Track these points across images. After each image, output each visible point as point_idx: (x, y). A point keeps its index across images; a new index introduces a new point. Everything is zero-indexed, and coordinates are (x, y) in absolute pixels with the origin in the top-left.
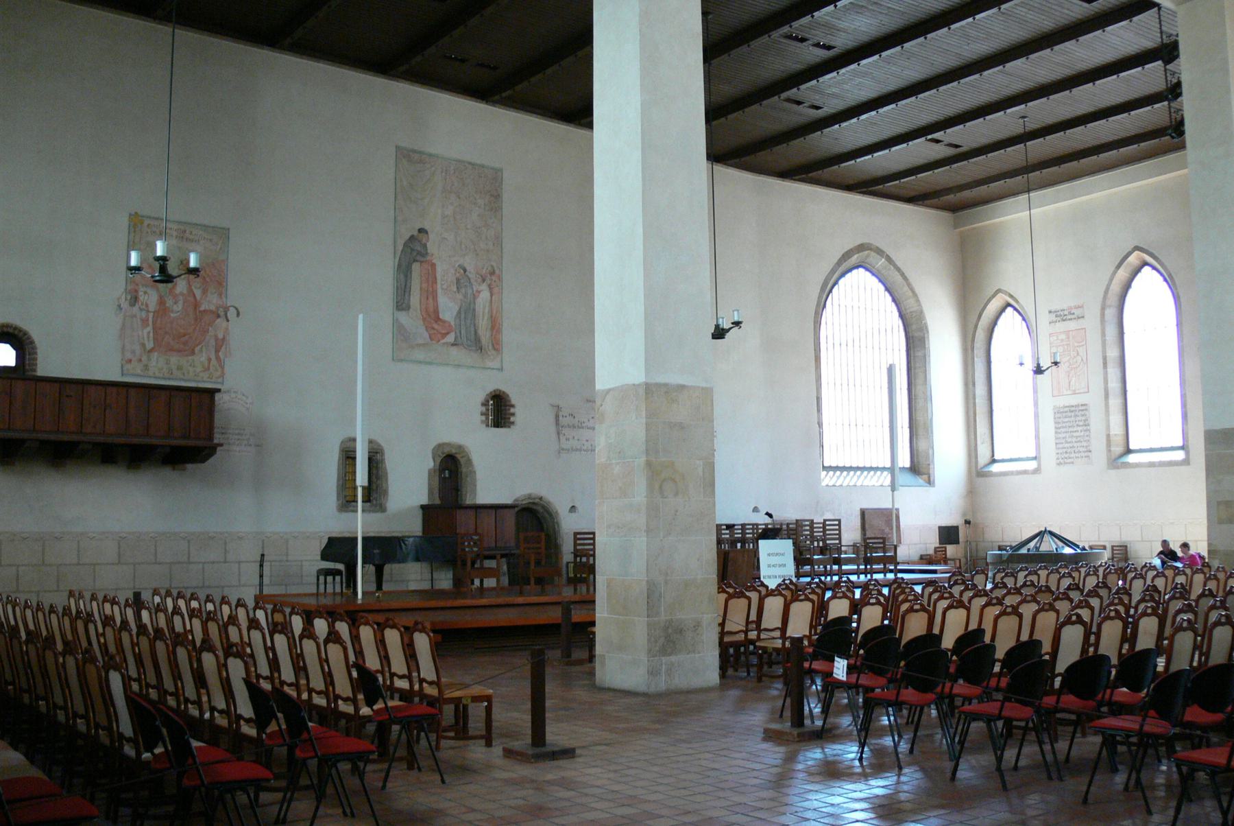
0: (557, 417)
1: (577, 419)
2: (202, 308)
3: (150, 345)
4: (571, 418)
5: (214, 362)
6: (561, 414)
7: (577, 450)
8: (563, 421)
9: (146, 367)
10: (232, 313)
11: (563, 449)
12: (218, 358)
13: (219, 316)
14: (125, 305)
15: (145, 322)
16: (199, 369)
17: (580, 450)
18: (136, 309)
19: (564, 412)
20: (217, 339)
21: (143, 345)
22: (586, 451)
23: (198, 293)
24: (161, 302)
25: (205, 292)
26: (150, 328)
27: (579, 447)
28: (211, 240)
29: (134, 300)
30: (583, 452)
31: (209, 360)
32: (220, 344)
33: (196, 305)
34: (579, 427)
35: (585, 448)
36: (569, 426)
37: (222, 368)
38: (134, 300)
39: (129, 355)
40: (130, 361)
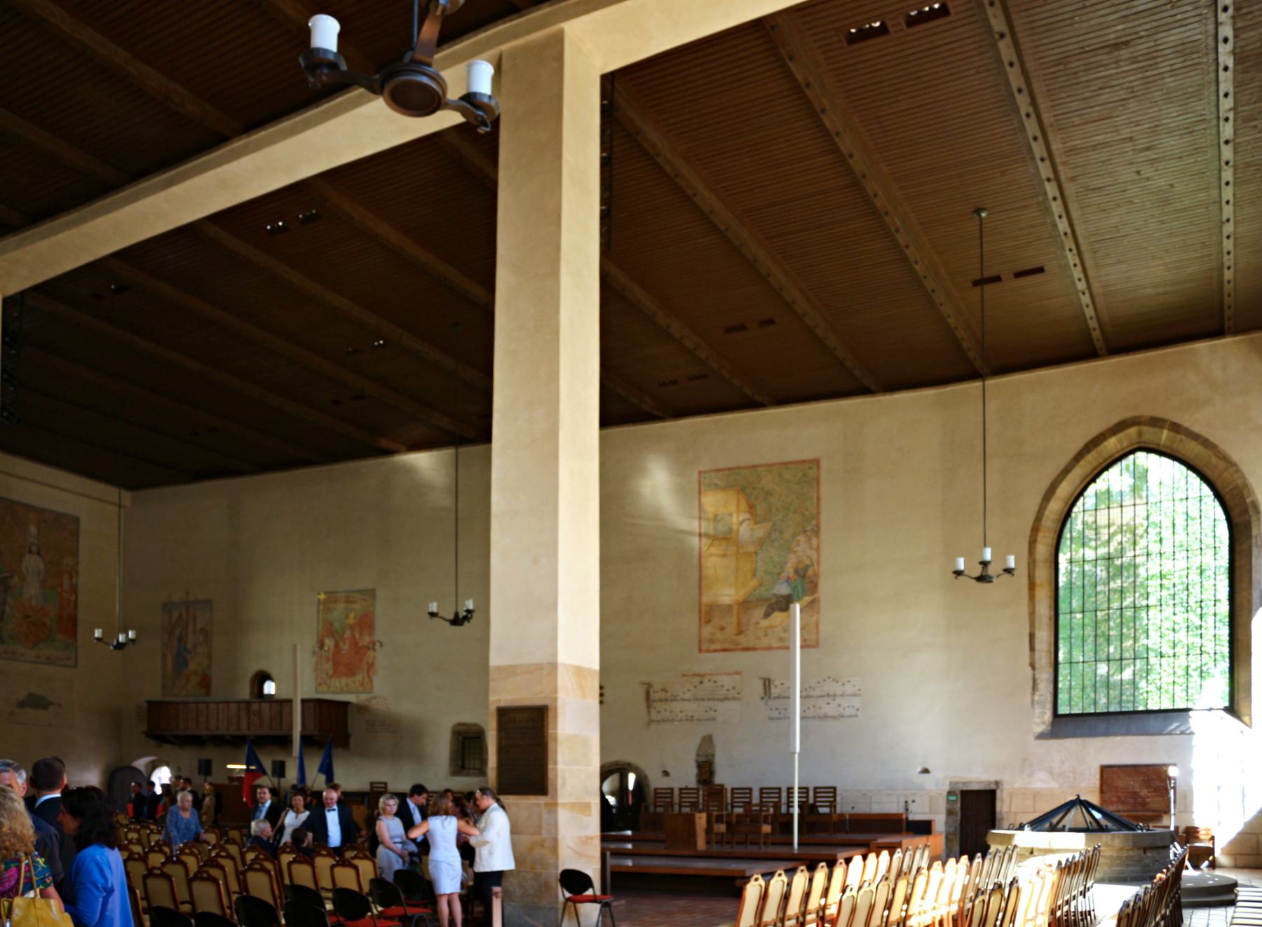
0: (648, 694)
1: (669, 694)
2: (361, 644)
3: (331, 672)
4: (664, 693)
5: (366, 680)
6: (652, 690)
7: (668, 721)
8: (653, 695)
9: (329, 687)
10: (377, 645)
11: (653, 721)
12: (369, 677)
13: (369, 649)
14: (317, 649)
15: (328, 660)
16: (358, 684)
17: (673, 720)
18: (323, 652)
19: (656, 687)
20: (368, 663)
21: (327, 674)
22: (681, 720)
23: (357, 635)
24: (337, 645)
25: (361, 634)
26: (330, 663)
27: (671, 718)
28: (364, 600)
29: (322, 645)
30: (676, 723)
31: (363, 678)
32: (371, 666)
33: (356, 643)
34: (672, 700)
35: (679, 718)
36: (661, 700)
37: (371, 682)
38: (322, 645)
39: (319, 681)
40: (320, 684)
